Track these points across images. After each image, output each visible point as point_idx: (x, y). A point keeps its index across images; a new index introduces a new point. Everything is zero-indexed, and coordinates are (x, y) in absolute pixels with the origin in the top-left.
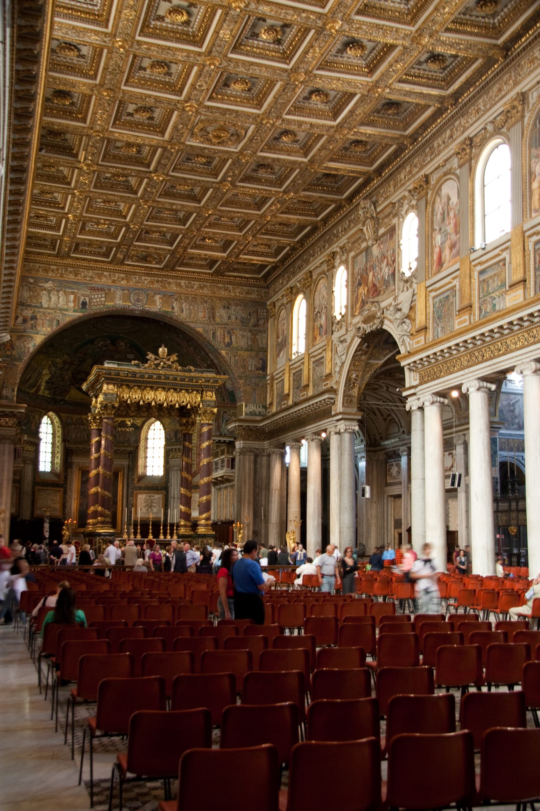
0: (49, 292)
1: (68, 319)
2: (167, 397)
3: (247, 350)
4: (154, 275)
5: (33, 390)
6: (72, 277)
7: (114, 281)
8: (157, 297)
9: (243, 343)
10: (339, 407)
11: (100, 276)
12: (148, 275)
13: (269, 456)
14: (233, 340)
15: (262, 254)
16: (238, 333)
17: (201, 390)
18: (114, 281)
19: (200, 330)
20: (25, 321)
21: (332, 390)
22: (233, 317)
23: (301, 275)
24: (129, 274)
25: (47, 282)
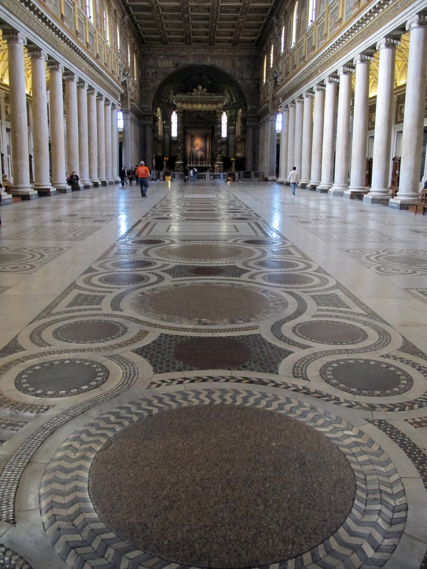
0: (162, 60)
1: (170, 72)
2: (202, 107)
3: (250, 80)
4: (207, 48)
5: (167, 100)
6: (170, 53)
7: (189, 53)
8: (208, 58)
9: (248, 76)
10: (270, 110)
11: (182, 51)
12: (203, 48)
13: (259, 128)
14: (244, 76)
15: (250, 36)
16: (245, 71)
17: (216, 103)
18: (189, 53)
19: (228, 72)
20: (152, 74)
21: (268, 102)
22: (243, 65)
23: (265, 46)
24: (195, 49)
25: (160, 55)
